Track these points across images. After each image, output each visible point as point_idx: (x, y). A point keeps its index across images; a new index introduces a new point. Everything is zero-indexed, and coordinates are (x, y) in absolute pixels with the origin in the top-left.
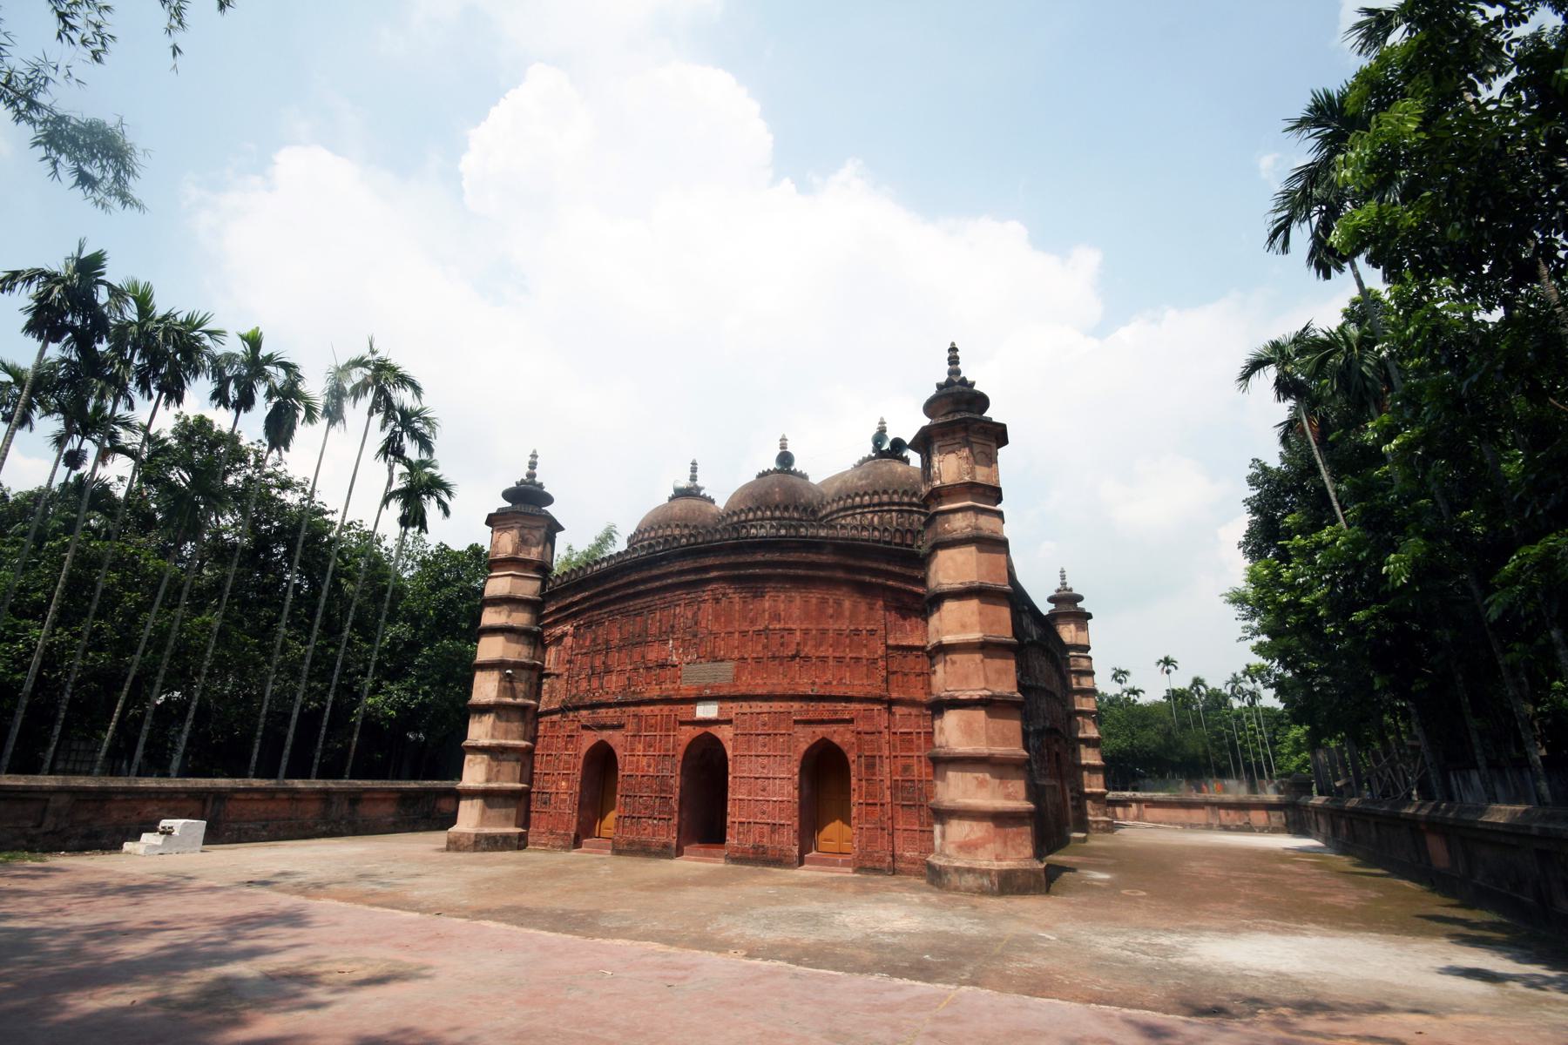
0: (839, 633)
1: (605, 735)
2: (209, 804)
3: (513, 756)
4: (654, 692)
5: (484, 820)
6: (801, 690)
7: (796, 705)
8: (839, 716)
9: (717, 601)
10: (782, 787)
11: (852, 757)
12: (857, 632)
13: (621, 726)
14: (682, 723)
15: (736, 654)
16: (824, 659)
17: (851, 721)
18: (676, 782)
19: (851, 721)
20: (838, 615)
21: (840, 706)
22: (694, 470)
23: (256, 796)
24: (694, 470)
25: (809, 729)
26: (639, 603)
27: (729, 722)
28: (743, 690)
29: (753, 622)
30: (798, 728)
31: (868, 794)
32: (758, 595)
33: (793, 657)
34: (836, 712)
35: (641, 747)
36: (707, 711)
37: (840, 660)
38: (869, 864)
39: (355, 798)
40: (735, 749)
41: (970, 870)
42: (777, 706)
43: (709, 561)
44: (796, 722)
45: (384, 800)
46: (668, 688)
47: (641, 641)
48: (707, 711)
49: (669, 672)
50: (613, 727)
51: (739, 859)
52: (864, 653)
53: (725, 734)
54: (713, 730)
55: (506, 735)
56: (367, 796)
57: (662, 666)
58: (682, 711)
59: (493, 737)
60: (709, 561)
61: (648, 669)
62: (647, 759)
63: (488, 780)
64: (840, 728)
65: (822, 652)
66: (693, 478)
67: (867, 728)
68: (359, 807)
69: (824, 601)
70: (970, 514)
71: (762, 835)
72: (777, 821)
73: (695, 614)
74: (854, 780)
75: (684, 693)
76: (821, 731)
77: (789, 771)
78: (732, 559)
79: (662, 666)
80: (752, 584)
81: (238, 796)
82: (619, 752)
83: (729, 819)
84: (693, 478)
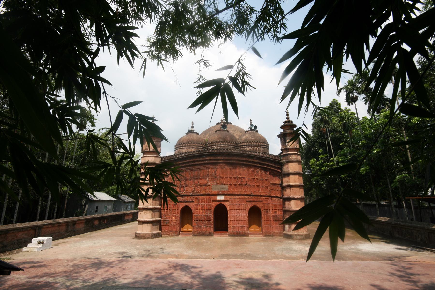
0: (258, 179)
1: (187, 204)
2: (37, 231)
3: (157, 210)
4: (204, 193)
5: (152, 230)
6: (248, 193)
7: (247, 197)
8: (259, 200)
9: (222, 169)
10: (244, 217)
11: (262, 210)
12: (262, 179)
13: (193, 202)
14: (213, 201)
15: (229, 183)
16: (254, 186)
17: (262, 201)
18: (212, 217)
19: (262, 201)
20: (257, 175)
21: (259, 197)
22: (193, 124)
23: (50, 226)
24: (193, 124)
25: (250, 203)
26: (196, 167)
27: (228, 201)
28: (231, 193)
29: (233, 175)
30: (247, 203)
31: (267, 218)
32: (235, 168)
33: (245, 185)
34: (258, 199)
35: (200, 207)
36: (220, 198)
37: (258, 186)
38: (267, 234)
39: (74, 223)
40: (230, 208)
41: (298, 235)
42: (241, 197)
43: (220, 158)
44: (247, 201)
45: (81, 223)
46: (208, 191)
47: (198, 178)
48: (220, 198)
49: (207, 187)
50: (190, 202)
51: (231, 235)
52: (264, 185)
53: (227, 204)
54: (222, 203)
55: (155, 205)
56: (78, 222)
57: (206, 185)
58: (213, 198)
59: (152, 205)
60: (220, 158)
61: (200, 186)
62: (202, 210)
63: (152, 218)
64: (259, 203)
65: (253, 184)
66: (192, 127)
67: (265, 203)
68: (75, 226)
69: (253, 171)
70: (296, 155)
71: (238, 229)
72: (243, 225)
73: (215, 172)
74: (263, 215)
75: (213, 193)
76: (254, 204)
77: (246, 213)
78: (227, 158)
79: (206, 185)
80: (233, 165)
81: (45, 227)
82: (192, 209)
83: (229, 226)
84: (192, 127)
